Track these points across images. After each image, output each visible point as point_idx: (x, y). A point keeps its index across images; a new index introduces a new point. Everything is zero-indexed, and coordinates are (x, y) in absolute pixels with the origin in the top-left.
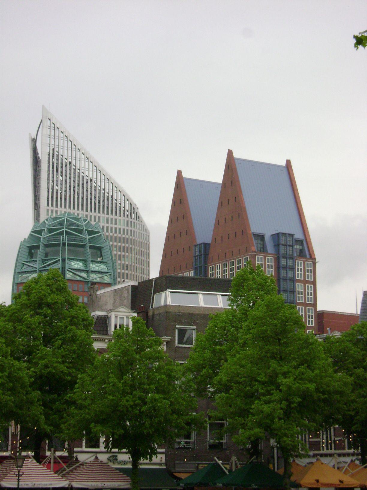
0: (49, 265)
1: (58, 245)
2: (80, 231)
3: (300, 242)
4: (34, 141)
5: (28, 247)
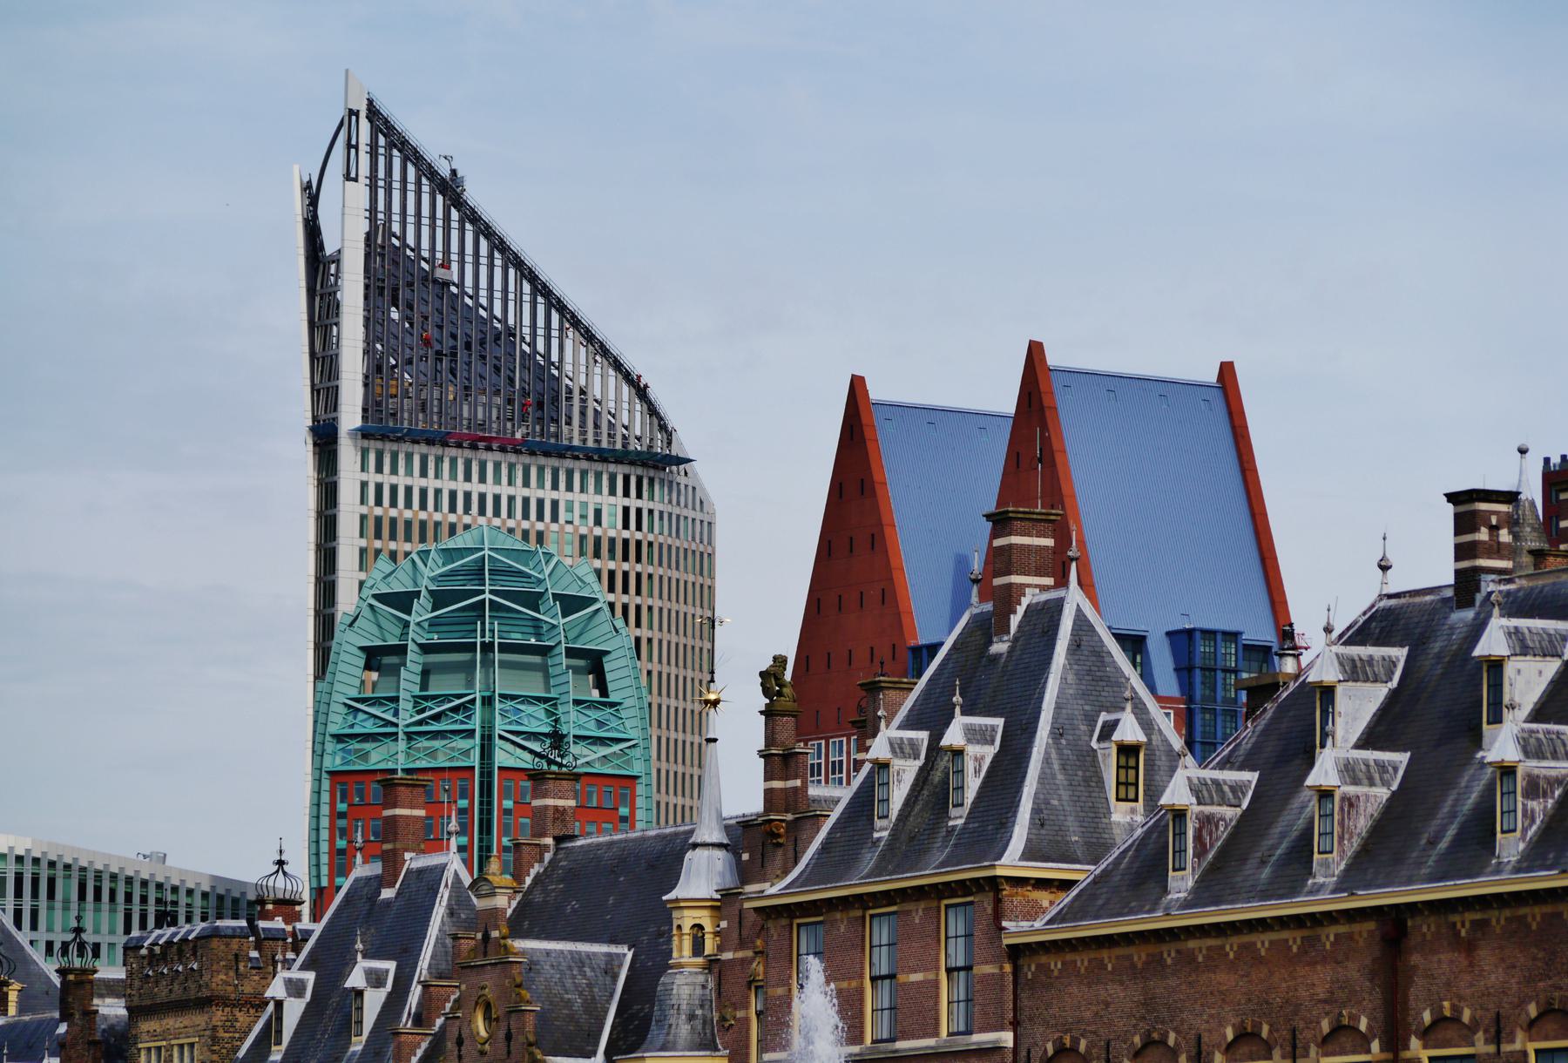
0: (437, 718)
1: (471, 648)
2: (533, 600)
3: (1261, 653)
4: (312, 196)
5: (362, 649)
